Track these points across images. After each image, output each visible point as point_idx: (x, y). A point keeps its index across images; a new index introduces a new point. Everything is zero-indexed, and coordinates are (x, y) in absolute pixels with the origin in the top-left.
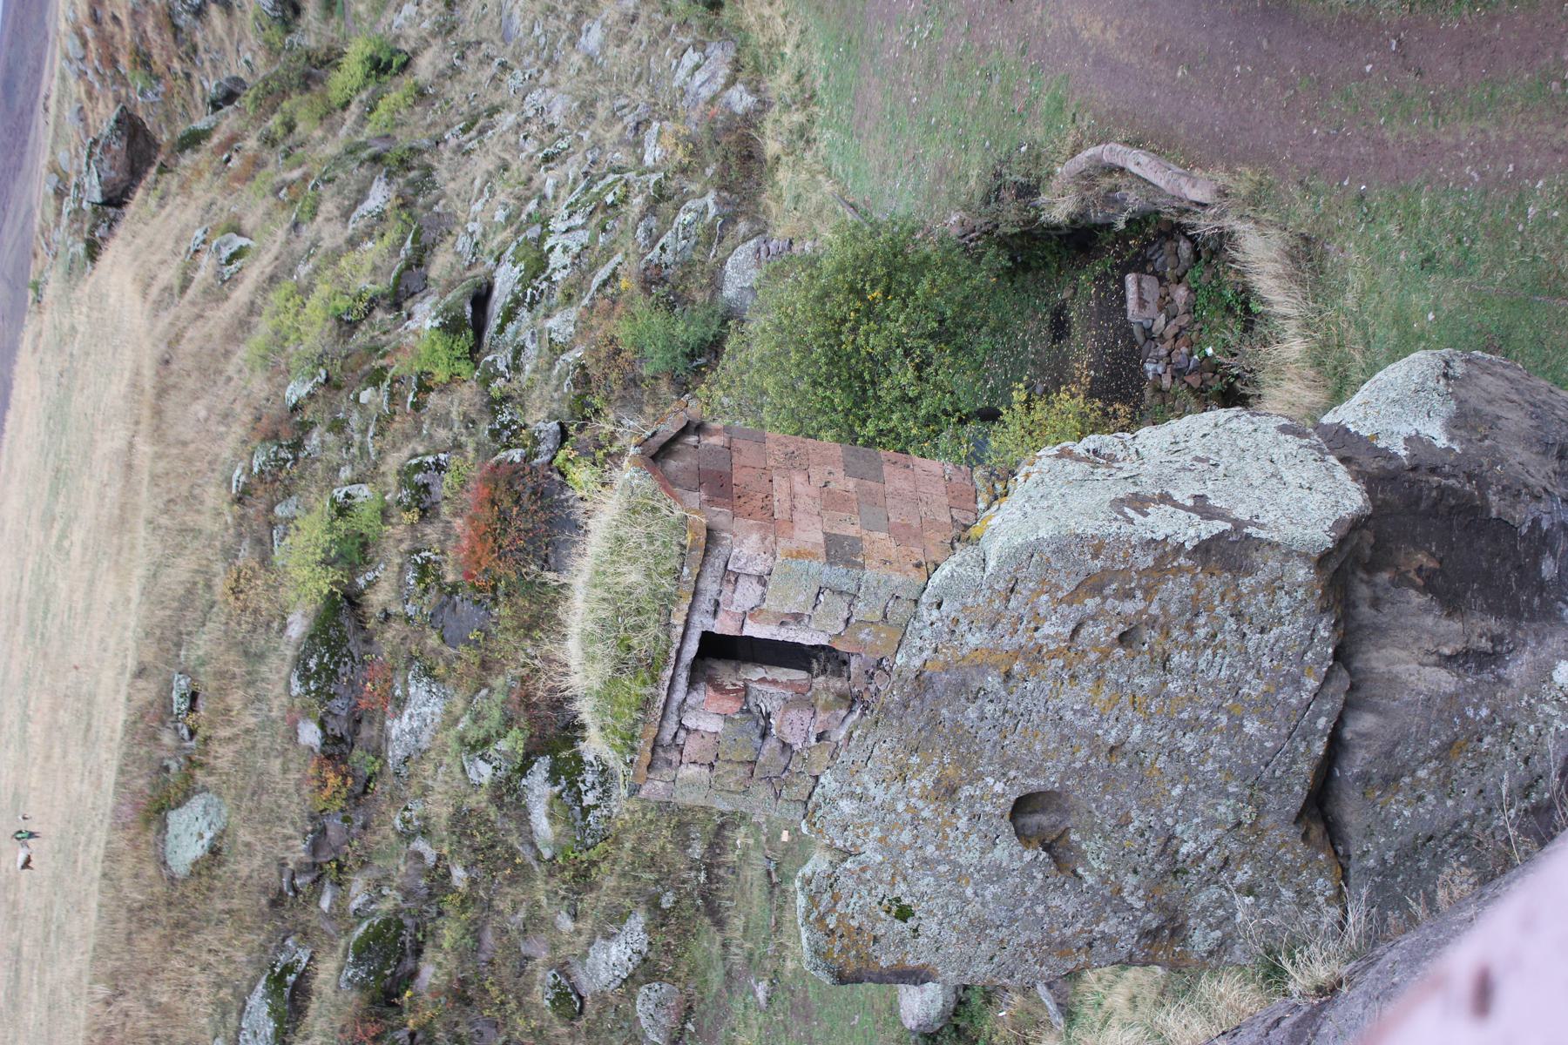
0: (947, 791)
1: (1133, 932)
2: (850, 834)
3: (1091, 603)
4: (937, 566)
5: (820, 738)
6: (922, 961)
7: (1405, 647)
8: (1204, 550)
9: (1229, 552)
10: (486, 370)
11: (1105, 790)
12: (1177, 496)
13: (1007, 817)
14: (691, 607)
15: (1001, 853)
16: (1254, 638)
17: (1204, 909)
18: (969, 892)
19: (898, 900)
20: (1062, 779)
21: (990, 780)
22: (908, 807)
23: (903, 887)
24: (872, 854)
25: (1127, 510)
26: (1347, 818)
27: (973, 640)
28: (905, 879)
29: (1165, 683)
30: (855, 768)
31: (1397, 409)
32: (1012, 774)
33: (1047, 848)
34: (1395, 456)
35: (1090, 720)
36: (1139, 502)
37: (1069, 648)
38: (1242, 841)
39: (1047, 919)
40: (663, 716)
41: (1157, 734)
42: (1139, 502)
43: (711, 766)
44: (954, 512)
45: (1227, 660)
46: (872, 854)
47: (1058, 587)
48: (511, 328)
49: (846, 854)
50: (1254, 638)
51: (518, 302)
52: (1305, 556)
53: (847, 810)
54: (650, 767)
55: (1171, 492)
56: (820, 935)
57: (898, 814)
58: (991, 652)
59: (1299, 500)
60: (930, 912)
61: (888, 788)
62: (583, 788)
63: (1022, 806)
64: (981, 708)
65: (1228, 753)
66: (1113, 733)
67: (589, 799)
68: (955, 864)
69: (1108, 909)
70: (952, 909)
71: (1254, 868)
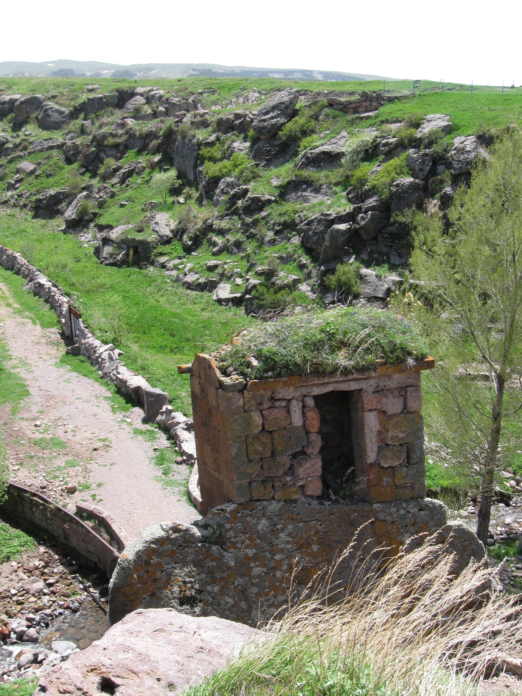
23: (216, 589)
28: (222, 588)
30: (294, 516)
53: (260, 527)
57: (272, 558)
61: (288, 542)
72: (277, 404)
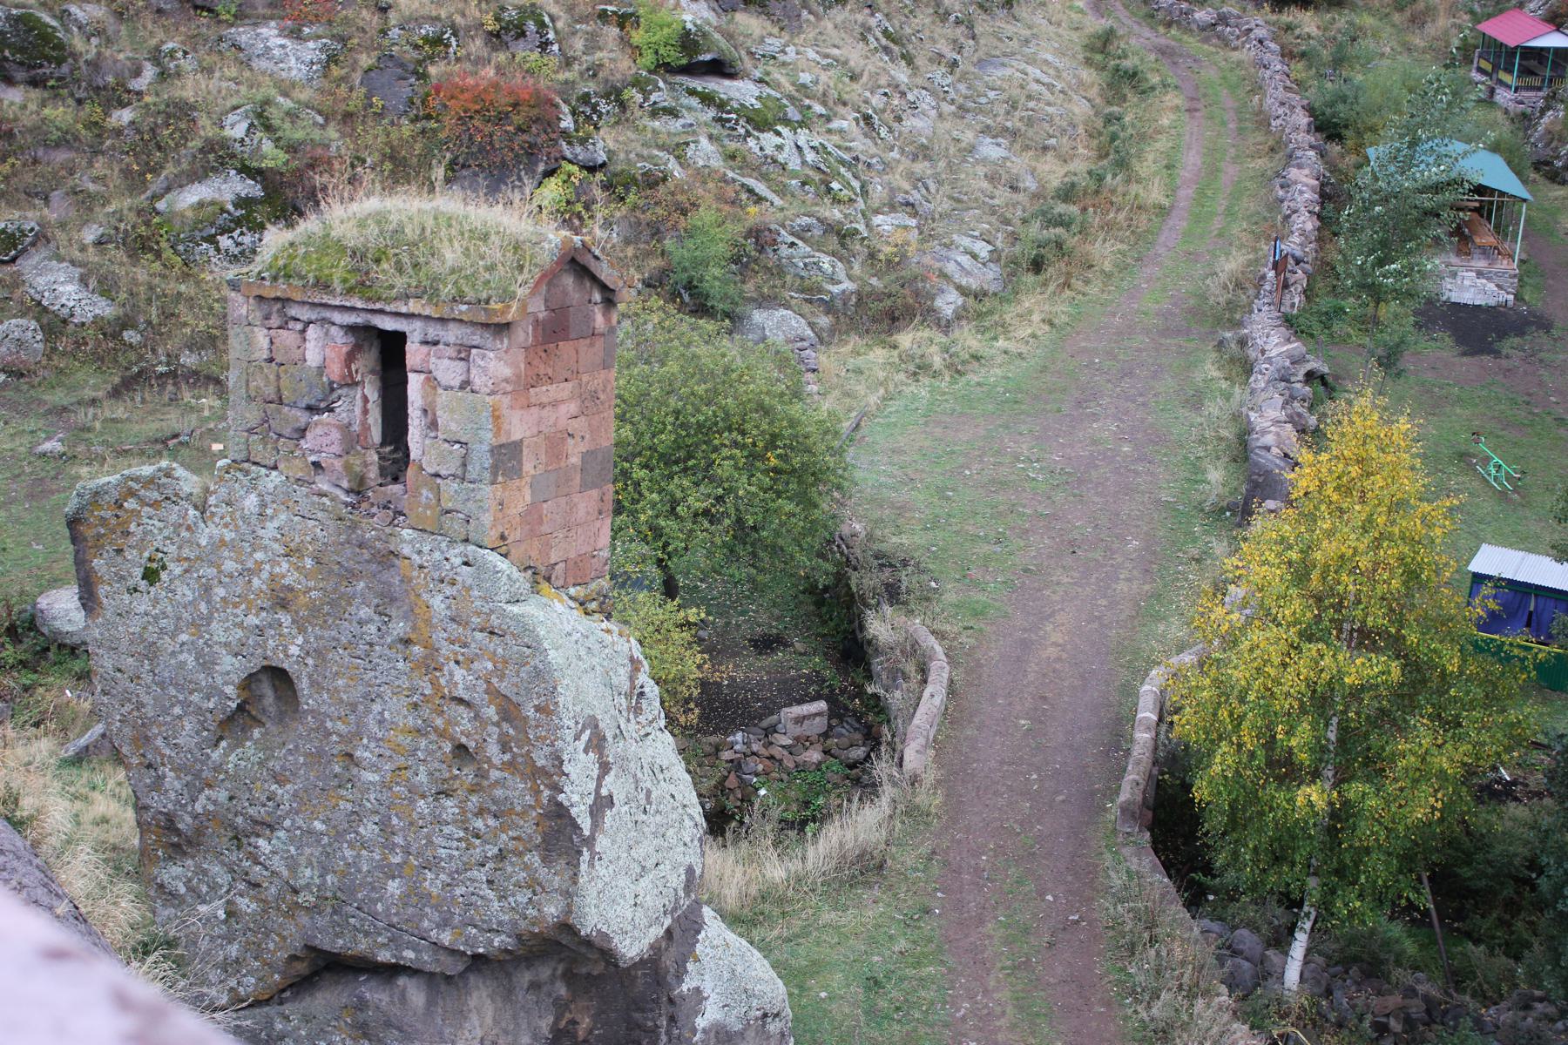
0: (282, 599)
1: (170, 806)
2: (224, 509)
3: (491, 712)
4: (505, 556)
5: (316, 465)
6: (105, 601)
7: (496, 1022)
8: (560, 813)
9: (561, 836)
10: (648, 82)
11: (308, 755)
12: (609, 779)
13: (265, 663)
14: (428, 318)
15: (228, 662)
16: (481, 875)
17: (205, 872)
18: (184, 637)
19: (164, 568)
20: (312, 711)
21: (300, 640)
22: (259, 564)
23: (178, 571)
24: (206, 534)
25: (588, 732)
26: (319, 995)
27: (437, 602)
28: (186, 571)
29: (423, 797)
31: (726, 975)
32: (310, 661)
33: (240, 708)
34: (680, 979)
35: (376, 729)
36: (597, 743)
37: (443, 697)
38: (279, 897)
39: (168, 719)
40: (314, 305)
41: (372, 797)
42: (597, 743)
43: (271, 360)
44: (562, 565)
45: (456, 853)
46: (206, 534)
47: (502, 677)
48: (694, 102)
49: (202, 508)
50: (481, 875)
51: (722, 106)
52: (569, 911)
53: (247, 503)
54: (260, 298)
55: (612, 773)
56: (115, 494)
57: (251, 554)
58: (428, 622)
59: (623, 896)
60: (156, 601)
61: (276, 540)
62: (235, 234)
63: (279, 677)
64: (370, 621)
65: (365, 869)
66: (367, 754)
67: (225, 242)
68: (209, 619)
69: (189, 778)
70: (163, 623)
71: (254, 914)
72: (291, 324)
